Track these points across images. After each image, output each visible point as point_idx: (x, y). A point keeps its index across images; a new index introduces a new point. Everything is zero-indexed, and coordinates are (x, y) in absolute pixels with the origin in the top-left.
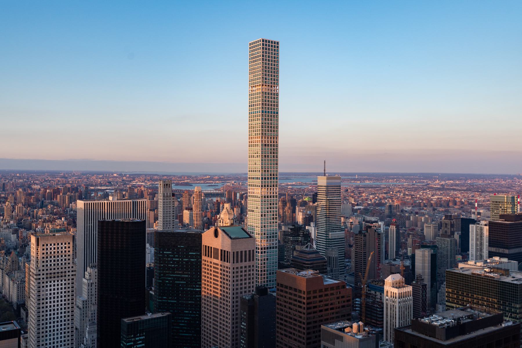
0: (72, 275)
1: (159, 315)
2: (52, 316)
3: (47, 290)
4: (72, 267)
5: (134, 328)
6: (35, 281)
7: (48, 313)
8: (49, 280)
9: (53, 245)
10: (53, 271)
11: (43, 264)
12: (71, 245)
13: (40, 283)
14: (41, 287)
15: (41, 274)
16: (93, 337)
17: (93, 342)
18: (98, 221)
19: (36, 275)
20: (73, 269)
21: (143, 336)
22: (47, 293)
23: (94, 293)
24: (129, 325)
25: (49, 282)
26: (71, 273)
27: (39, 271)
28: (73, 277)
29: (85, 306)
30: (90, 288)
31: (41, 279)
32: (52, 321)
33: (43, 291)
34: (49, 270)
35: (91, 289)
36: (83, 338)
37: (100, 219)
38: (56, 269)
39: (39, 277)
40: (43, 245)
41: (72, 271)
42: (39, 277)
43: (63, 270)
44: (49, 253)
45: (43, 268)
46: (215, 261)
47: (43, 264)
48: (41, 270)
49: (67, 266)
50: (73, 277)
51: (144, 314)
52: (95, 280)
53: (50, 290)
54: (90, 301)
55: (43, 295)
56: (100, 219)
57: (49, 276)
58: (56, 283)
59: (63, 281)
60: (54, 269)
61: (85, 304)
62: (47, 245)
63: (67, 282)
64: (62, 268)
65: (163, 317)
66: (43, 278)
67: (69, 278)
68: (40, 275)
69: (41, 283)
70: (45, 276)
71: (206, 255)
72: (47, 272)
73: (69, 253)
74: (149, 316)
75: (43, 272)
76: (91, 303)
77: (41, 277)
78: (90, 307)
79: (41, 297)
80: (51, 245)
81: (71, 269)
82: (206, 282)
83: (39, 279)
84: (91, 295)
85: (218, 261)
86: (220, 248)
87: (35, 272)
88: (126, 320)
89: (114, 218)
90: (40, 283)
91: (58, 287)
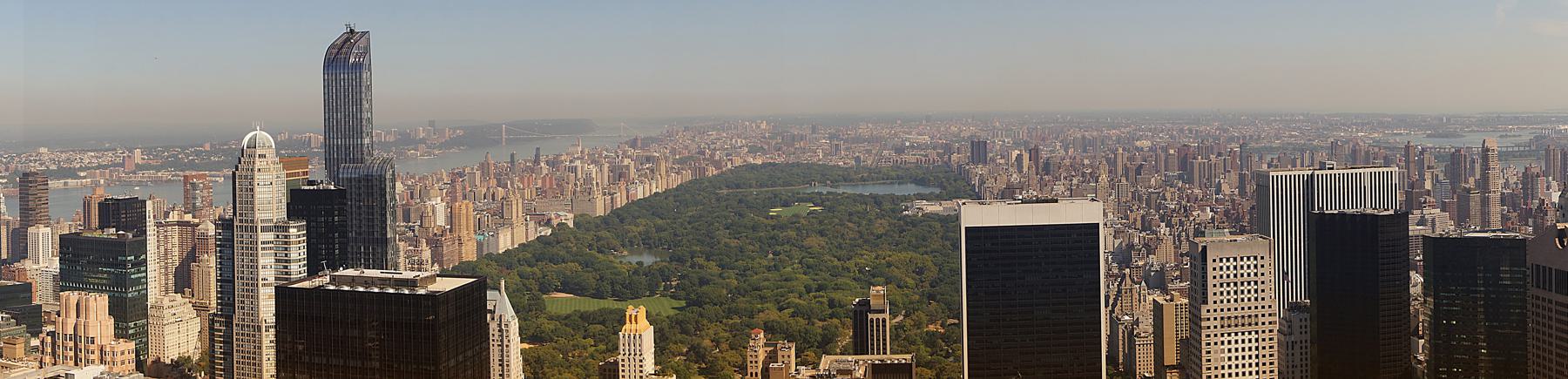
0: (1270, 323)
4: (1270, 307)
10: (1233, 313)
11: (1215, 298)
15: (1212, 319)
20: (1270, 311)
22: (1222, 355)
26: (1267, 319)
27: (1208, 311)
28: (1271, 327)
33: (1216, 352)
41: (1270, 315)
43: (1253, 312)
45: (1215, 306)
47: (1215, 298)
48: (1212, 311)
49: (1260, 303)
50: (1271, 327)
53: (1230, 350)
57: (1226, 322)
58: (1240, 337)
62: (1221, 260)
63: (1262, 336)
67: (1264, 328)
68: (1209, 319)
69: (1212, 336)
70: (1218, 323)
72: (1222, 314)
73: (1263, 279)
75: (1215, 315)
77: (1212, 323)
80: (1228, 260)
81: (1267, 311)
83: (1209, 328)
89: (1340, 208)
91: (1243, 345)
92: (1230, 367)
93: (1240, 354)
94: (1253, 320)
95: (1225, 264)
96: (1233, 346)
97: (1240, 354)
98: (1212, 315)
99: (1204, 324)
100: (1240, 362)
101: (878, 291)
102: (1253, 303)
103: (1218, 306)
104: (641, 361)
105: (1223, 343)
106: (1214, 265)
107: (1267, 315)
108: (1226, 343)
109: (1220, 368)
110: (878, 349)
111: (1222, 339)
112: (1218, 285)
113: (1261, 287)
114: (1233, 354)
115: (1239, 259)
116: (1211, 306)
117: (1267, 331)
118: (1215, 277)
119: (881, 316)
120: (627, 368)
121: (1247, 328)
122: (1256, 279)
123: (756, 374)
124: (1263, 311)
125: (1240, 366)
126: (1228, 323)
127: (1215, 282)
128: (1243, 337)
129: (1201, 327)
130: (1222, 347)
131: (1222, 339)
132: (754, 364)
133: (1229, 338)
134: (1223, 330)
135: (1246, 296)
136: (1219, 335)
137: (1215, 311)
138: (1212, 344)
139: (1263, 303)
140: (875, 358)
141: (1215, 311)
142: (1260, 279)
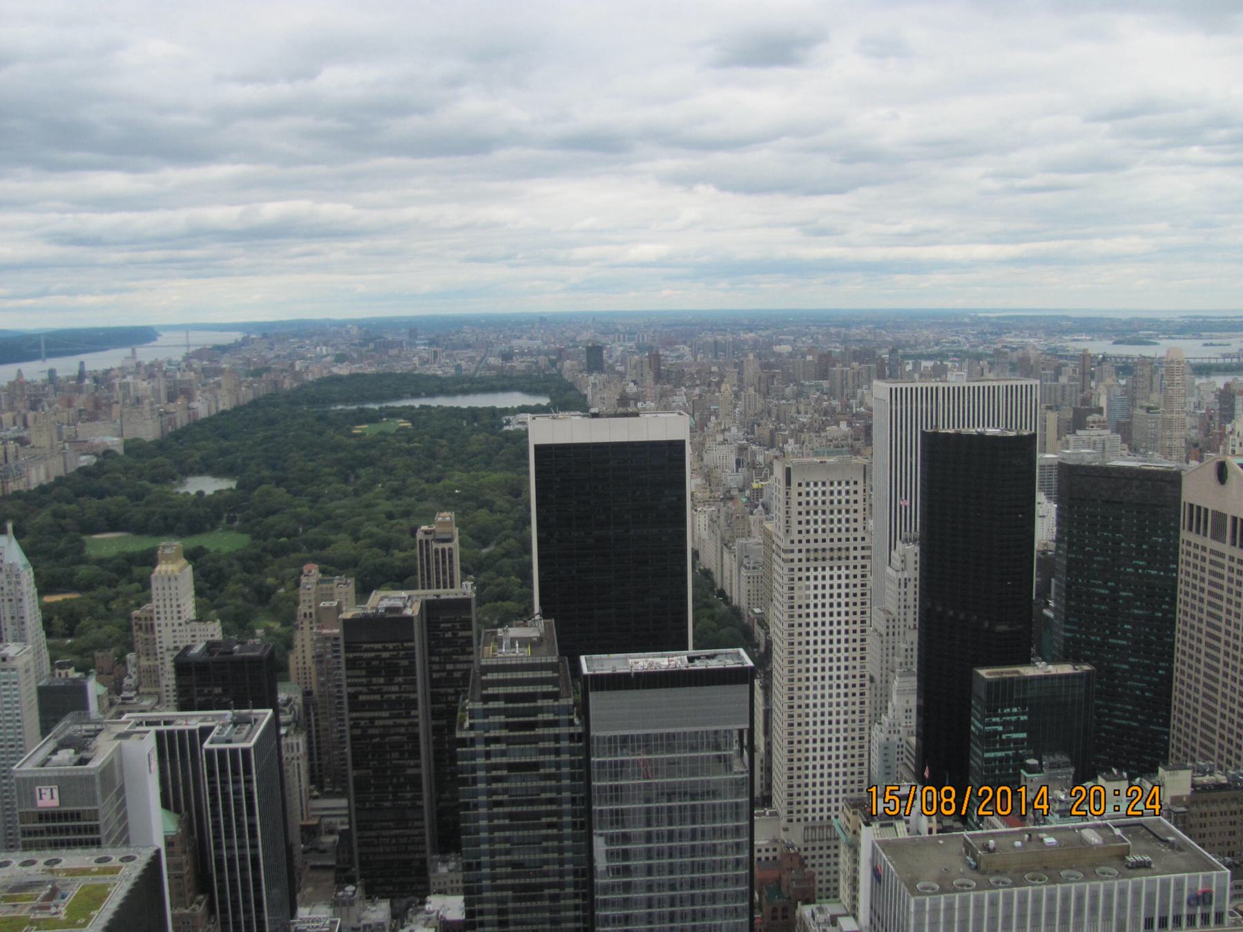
0: (863, 557)
1: (1066, 669)
2: (819, 647)
3: (808, 588)
4: (863, 539)
5: (1003, 693)
6: (782, 563)
8: (812, 564)
9: (820, 484)
10: (820, 545)
11: (800, 527)
12: (860, 488)
13: (792, 570)
16: (908, 702)
17: (909, 714)
18: (922, 432)
19: (785, 551)
21: (1024, 714)
22: (807, 592)
23: (911, 602)
24: (989, 684)
26: (859, 553)
27: (792, 542)
29: (891, 630)
30: (903, 590)
32: (819, 656)
33: (800, 588)
34: (812, 541)
35: (905, 593)
36: (887, 702)
37: (927, 427)
38: (828, 540)
39: (791, 556)
40: (800, 485)
41: (863, 548)
42: (791, 556)
43: (843, 544)
44: (812, 503)
45: (800, 537)
46: (1217, 546)
47: (800, 527)
48: (796, 542)
49: (851, 535)
50: (864, 562)
51: (1027, 661)
52: (913, 572)
53: (816, 587)
55: (800, 597)
56: (927, 427)
57: (812, 555)
58: (828, 573)
59: (843, 568)
60: (824, 541)
61: (891, 627)
62: (808, 485)
63: (851, 572)
66: (800, 560)
68: (792, 551)
69: (796, 570)
71: (1190, 529)
73: (855, 506)
74: (1039, 669)
76: (905, 626)
77: (796, 556)
78: (902, 633)
79: (796, 602)
80: (816, 484)
81: (859, 544)
82: (1189, 599)
83: (792, 560)
84: (905, 607)
85: (1226, 548)
86: (1230, 512)
87: (782, 546)
88: (983, 672)
90: (792, 570)
92: (816, 606)
93: (827, 591)
94: (843, 554)
95: (812, 489)
96: (820, 582)
97: (827, 591)
98: (796, 546)
100: (827, 601)
101: (444, 517)
102: (843, 535)
103: (804, 537)
104: (178, 606)
105: (808, 578)
106: (800, 489)
107: (859, 548)
108: (812, 578)
109: (804, 607)
110: (445, 583)
112: (804, 513)
113: (852, 516)
114: (820, 592)
115: (828, 484)
117: (859, 567)
119: (446, 546)
120: (162, 616)
121: (836, 563)
122: (848, 507)
123: (311, 614)
124: (855, 544)
125: (827, 605)
127: (800, 509)
130: (807, 583)
131: (807, 574)
133: (815, 573)
134: (808, 565)
135: (836, 526)
136: (804, 569)
137: (800, 541)
138: (796, 579)
139: (855, 535)
140: (430, 594)
141: (800, 541)
142: (852, 506)
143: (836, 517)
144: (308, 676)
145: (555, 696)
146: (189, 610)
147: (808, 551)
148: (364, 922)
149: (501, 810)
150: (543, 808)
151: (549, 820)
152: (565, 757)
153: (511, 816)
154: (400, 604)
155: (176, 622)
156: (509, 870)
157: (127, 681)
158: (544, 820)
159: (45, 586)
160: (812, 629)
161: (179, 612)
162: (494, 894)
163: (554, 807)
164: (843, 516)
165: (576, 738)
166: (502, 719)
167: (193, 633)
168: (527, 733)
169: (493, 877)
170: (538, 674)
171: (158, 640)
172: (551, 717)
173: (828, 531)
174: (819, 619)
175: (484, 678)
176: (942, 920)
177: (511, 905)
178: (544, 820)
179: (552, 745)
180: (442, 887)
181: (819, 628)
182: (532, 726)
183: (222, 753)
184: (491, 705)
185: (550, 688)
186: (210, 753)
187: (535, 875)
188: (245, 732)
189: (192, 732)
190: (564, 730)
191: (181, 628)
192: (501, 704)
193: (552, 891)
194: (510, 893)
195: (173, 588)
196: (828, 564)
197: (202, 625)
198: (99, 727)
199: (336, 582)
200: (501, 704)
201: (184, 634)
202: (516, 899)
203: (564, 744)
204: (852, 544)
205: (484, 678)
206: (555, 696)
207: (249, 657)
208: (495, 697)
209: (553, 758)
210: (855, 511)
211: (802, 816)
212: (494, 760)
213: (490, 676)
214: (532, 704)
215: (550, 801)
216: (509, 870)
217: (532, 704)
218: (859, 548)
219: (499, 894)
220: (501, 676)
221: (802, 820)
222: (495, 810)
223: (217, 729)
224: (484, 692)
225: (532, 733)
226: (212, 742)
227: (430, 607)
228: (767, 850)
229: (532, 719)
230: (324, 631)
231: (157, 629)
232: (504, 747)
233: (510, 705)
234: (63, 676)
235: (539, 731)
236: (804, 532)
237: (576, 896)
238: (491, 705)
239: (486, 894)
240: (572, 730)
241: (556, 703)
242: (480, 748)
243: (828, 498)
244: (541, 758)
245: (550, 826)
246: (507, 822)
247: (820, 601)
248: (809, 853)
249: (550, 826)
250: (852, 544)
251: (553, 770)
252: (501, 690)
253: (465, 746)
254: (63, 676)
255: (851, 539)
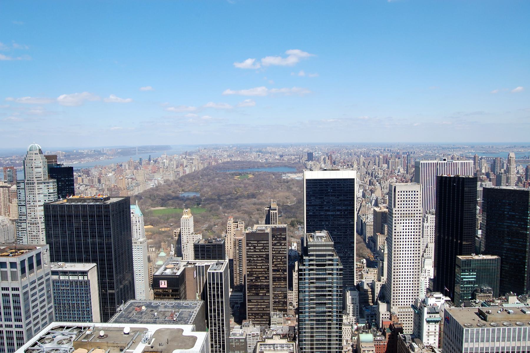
0: (420, 217)
2: (404, 246)
4: (420, 210)
7: (402, 243)
8: (402, 218)
9: (405, 192)
10: (405, 212)
13: (396, 220)
14: (397, 223)
15: (397, 214)
17: (429, 272)
21: (474, 272)
23: (429, 234)
25: (402, 220)
26: (418, 215)
27: (396, 211)
28: (420, 218)
30: (426, 230)
31: (397, 217)
32: (404, 249)
34: (402, 211)
35: (427, 231)
39: (395, 215)
41: (420, 214)
42: (395, 215)
43: (413, 212)
45: (398, 209)
48: (397, 211)
49: (416, 209)
50: (420, 218)
53: (403, 226)
54: (426, 240)
58: (407, 221)
59: (413, 220)
60: (406, 211)
62: (401, 192)
63: (416, 221)
64: (412, 211)
65: (493, 259)
68: (396, 214)
69: (397, 220)
73: (417, 199)
77: (397, 215)
80: (404, 192)
81: (418, 212)
83: (396, 217)
88: (460, 257)
92: (403, 232)
95: (403, 193)
96: (405, 225)
98: (397, 212)
99: (394, 215)
103: (400, 209)
104: (189, 229)
105: (401, 223)
107: (418, 214)
108: (402, 223)
109: (399, 232)
111: (401, 222)
112: (400, 201)
113: (416, 203)
114: (405, 228)
115: (408, 192)
116: (397, 209)
117: (418, 220)
118: (399, 198)
119: (275, 212)
122: (415, 199)
126: (404, 216)
127: (399, 200)
128: (409, 221)
129: (392, 217)
130: (401, 225)
131: (401, 222)
132: (229, 229)
133: (403, 222)
135: (410, 206)
136: (400, 220)
137: (398, 211)
138: (397, 223)
140: (273, 226)
141: (398, 211)
143: (410, 203)
144: (229, 253)
145: (332, 255)
146: (192, 230)
147: (401, 214)
148: (252, 333)
149: (313, 293)
150: (327, 293)
151: (329, 297)
152: (335, 276)
153: (317, 295)
154: (264, 228)
155: (188, 234)
156: (315, 314)
157: (171, 253)
158: (327, 297)
159: (146, 223)
160: (402, 240)
161: (189, 231)
162: (309, 322)
163: (331, 293)
164: (413, 203)
165: (339, 270)
166: (314, 263)
167: (193, 238)
168: (323, 268)
169: (309, 316)
170: (327, 248)
171: (182, 239)
172: (331, 262)
173: (408, 207)
174: (405, 237)
175: (309, 249)
176: (475, 337)
177: (315, 326)
178: (327, 297)
179: (331, 272)
180: (275, 322)
181: (404, 240)
182: (325, 265)
183: (213, 273)
184: (311, 258)
185: (331, 253)
186: (209, 273)
187: (324, 316)
188: (220, 267)
189: (203, 266)
190: (335, 267)
191: (189, 236)
192: (314, 258)
193: (329, 322)
194: (315, 322)
195: (187, 223)
196: (408, 218)
197: (196, 235)
198: (177, 263)
199: (239, 223)
200: (314, 258)
201: (190, 238)
202: (317, 324)
203: (335, 272)
204: (416, 212)
205: (309, 249)
206: (332, 255)
207: (218, 244)
208: (312, 255)
209: (331, 276)
210: (417, 201)
211: (398, 303)
212: (311, 276)
213: (311, 248)
214: (325, 258)
215: (330, 291)
216: (315, 314)
217: (325, 258)
218: (418, 214)
219: (311, 322)
220: (315, 248)
221: (398, 305)
222: (311, 293)
223: (211, 266)
224: (309, 253)
225: (324, 268)
226: (210, 270)
227: (273, 229)
228: (385, 315)
229: (324, 263)
230: (237, 238)
231: (182, 236)
232: (315, 272)
233: (317, 258)
234: (151, 250)
235: (327, 267)
236: (400, 208)
237: (337, 324)
238: (311, 258)
239: (306, 322)
240: (337, 267)
241: (333, 258)
242: (307, 272)
243: (408, 196)
244: (327, 276)
245: (329, 299)
246: (315, 297)
247: (405, 231)
248: (400, 317)
249: (329, 299)
250: (416, 212)
251: (331, 281)
252: (314, 253)
253: (302, 272)
254: (151, 250)
255: (416, 210)
